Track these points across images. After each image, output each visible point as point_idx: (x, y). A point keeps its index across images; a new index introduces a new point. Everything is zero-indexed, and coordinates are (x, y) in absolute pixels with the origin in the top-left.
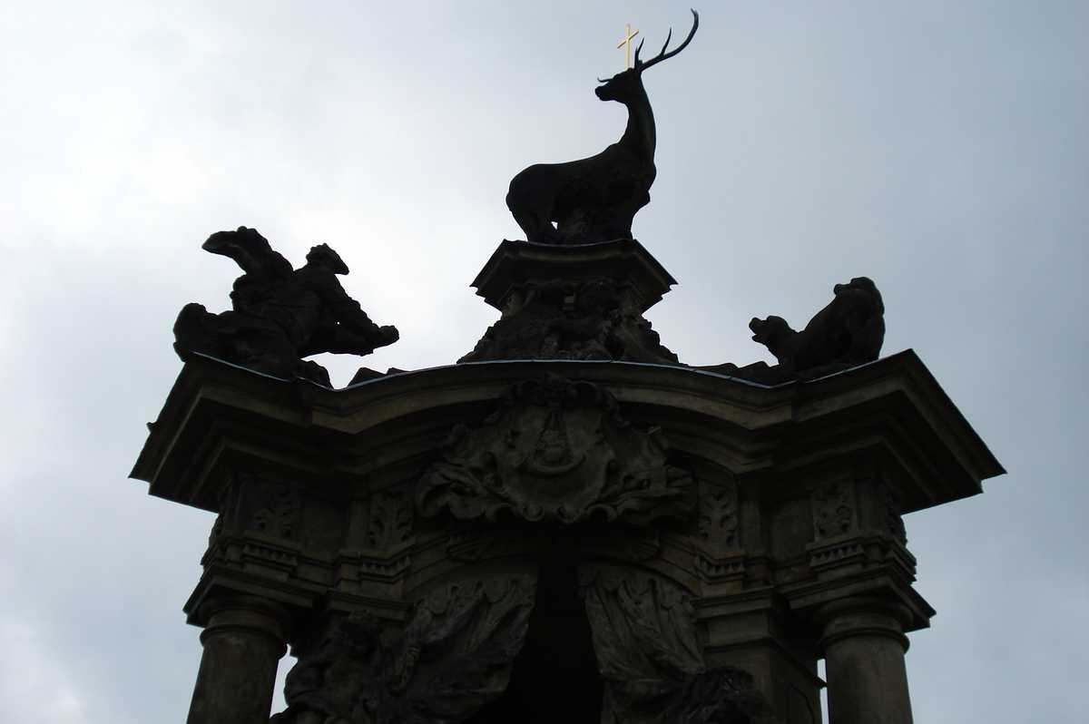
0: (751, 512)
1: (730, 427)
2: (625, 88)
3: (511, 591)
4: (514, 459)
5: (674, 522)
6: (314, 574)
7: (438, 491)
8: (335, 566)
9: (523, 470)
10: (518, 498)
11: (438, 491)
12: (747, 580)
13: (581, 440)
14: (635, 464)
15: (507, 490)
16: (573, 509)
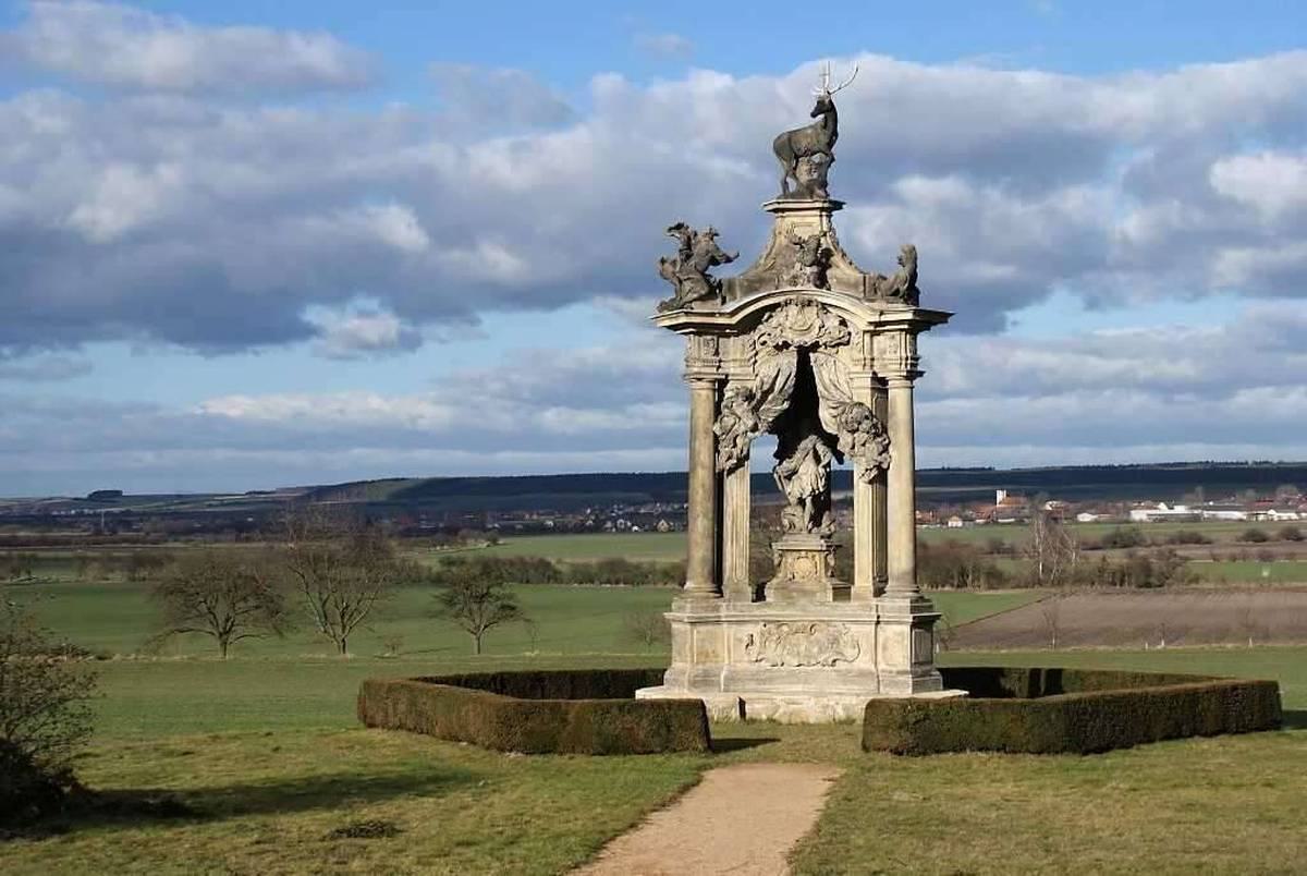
4: (788, 324)
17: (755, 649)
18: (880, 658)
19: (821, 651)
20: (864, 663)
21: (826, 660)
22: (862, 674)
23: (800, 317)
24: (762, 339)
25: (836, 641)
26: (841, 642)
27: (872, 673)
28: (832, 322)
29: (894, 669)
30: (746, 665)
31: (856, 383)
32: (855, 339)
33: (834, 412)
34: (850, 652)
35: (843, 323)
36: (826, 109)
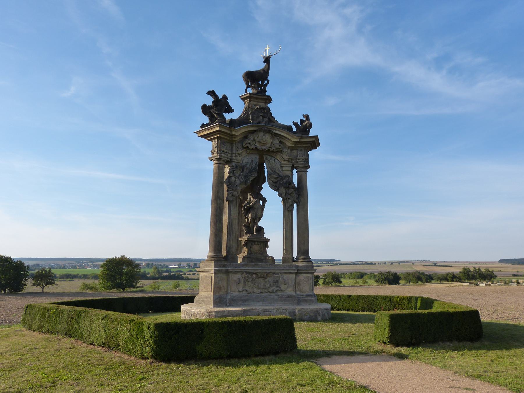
0: (289, 150)
1: (289, 140)
2: (267, 60)
3: (256, 158)
5: (279, 151)
6: (229, 155)
7: (246, 144)
8: (232, 154)
9: (259, 142)
10: (258, 145)
11: (246, 144)
12: (288, 161)
13: (268, 138)
14: (274, 142)
15: (256, 144)
16: (265, 148)
17: (241, 285)
18: (297, 289)
19: (271, 286)
20: (290, 291)
21: (273, 290)
22: (290, 296)
23: (264, 137)
24: (247, 145)
25: (277, 282)
26: (280, 282)
27: (294, 296)
28: (276, 142)
29: (305, 294)
30: (237, 293)
31: (284, 169)
32: (285, 150)
33: (275, 180)
34: (283, 287)
35: (281, 142)
36: (267, 60)
